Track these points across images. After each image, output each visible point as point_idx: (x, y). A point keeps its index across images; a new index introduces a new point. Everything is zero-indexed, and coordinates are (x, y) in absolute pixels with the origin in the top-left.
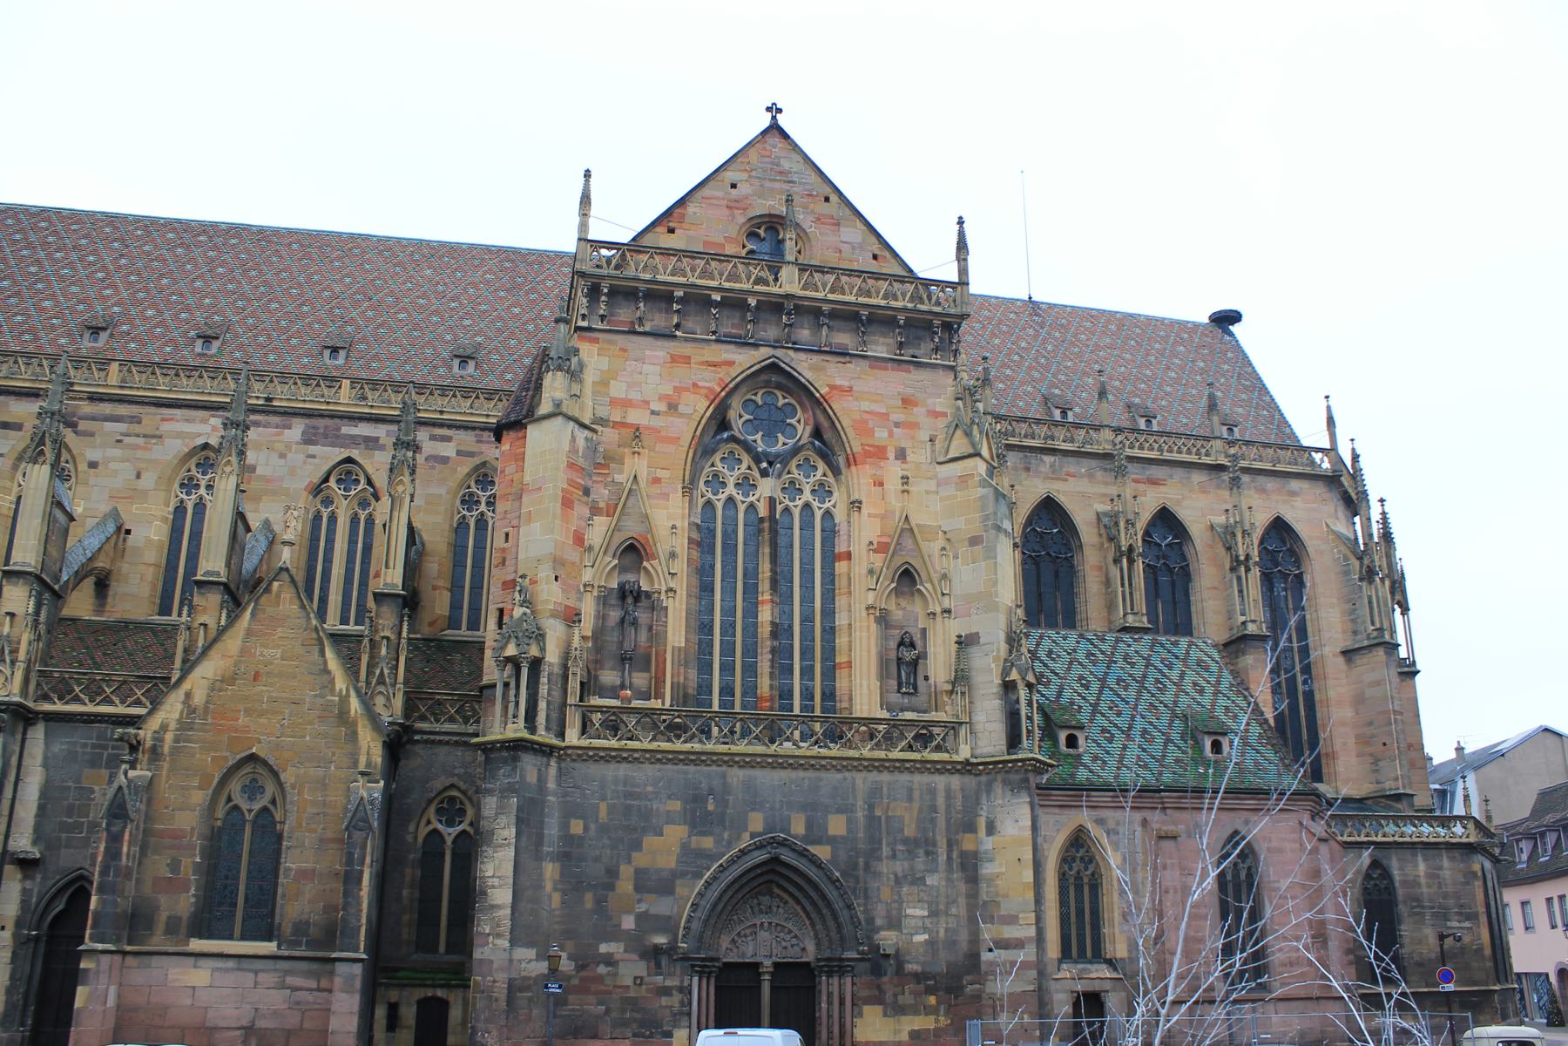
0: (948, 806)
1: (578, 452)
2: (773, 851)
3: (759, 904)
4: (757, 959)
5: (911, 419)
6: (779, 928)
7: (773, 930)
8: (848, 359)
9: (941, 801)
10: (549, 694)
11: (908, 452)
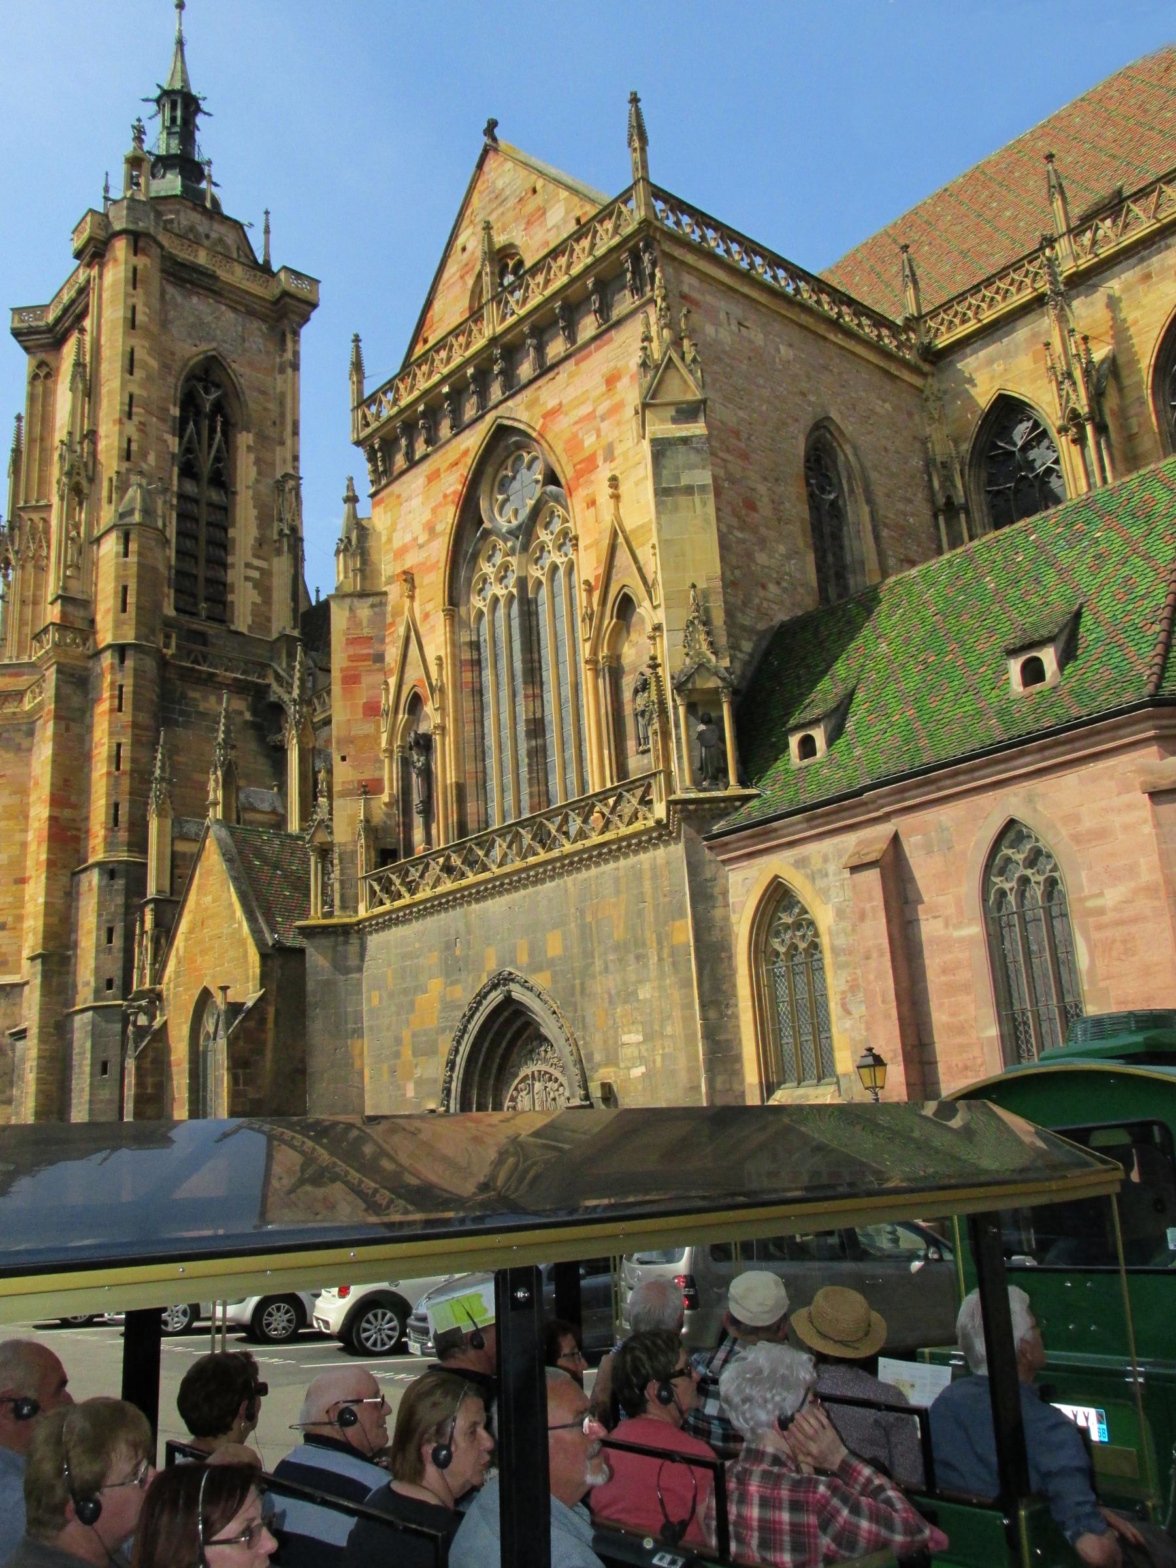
0: (655, 889)
1: (361, 624)
5: (617, 399)
8: (556, 371)
9: (647, 885)
10: (342, 874)
11: (616, 445)
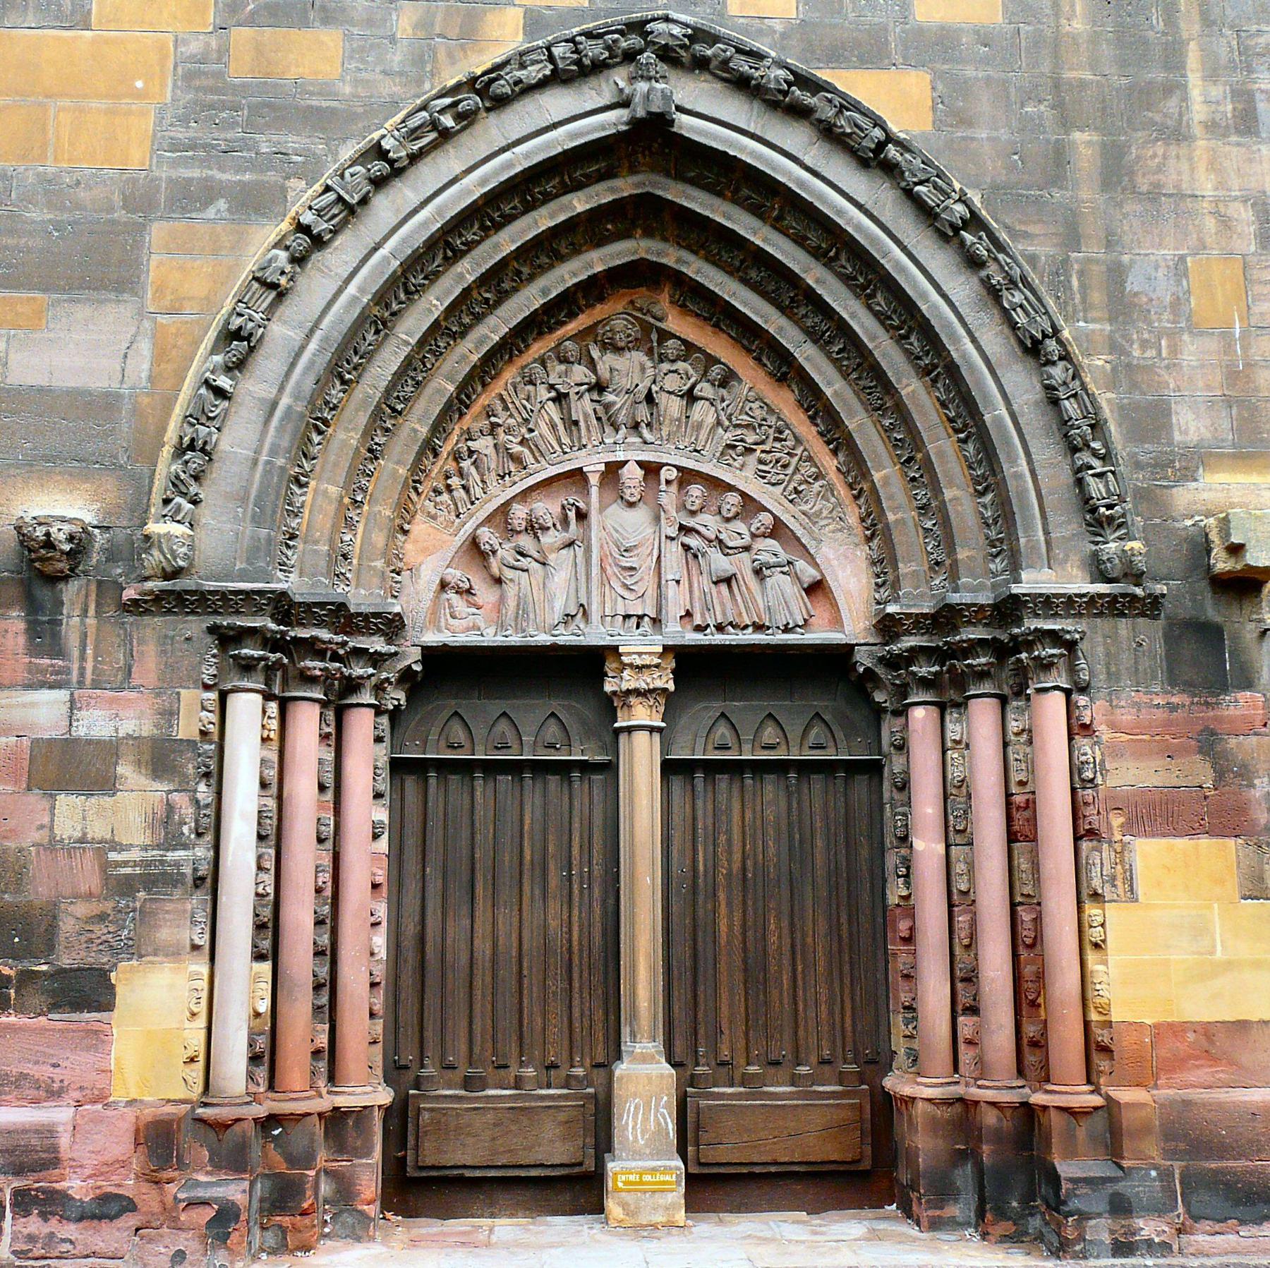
2: (642, 86)
3: (599, 387)
4: (594, 635)
6: (696, 490)
7: (669, 498)
